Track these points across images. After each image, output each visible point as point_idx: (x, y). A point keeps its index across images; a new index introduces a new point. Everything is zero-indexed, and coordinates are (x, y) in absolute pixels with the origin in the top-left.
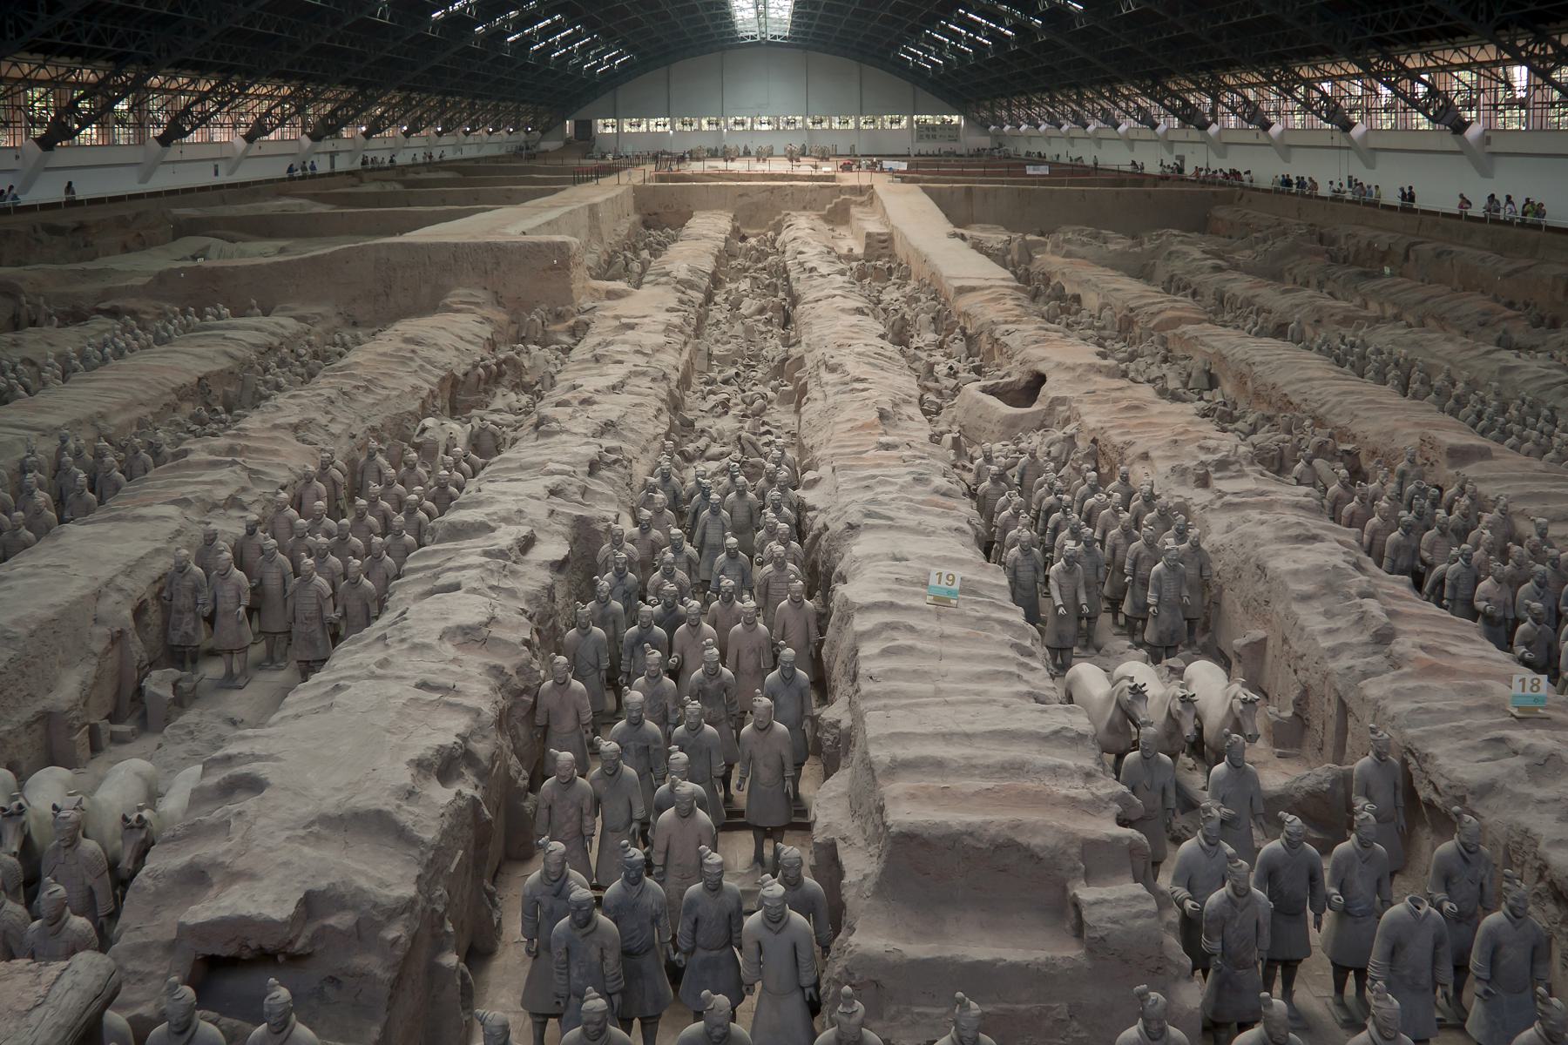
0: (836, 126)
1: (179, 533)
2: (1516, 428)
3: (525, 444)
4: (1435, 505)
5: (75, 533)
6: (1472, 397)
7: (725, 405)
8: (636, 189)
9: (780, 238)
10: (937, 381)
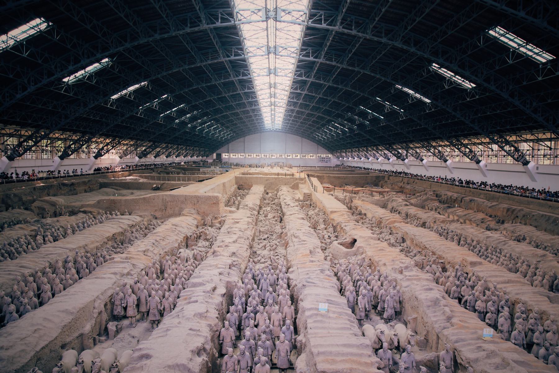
0: (294, 157)
1: (115, 283)
2: (490, 255)
3: (210, 258)
4: (465, 279)
5: (86, 283)
6: (478, 246)
7: (265, 247)
8: (236, 177)
9: (278, 194)
10: (325, 240)
